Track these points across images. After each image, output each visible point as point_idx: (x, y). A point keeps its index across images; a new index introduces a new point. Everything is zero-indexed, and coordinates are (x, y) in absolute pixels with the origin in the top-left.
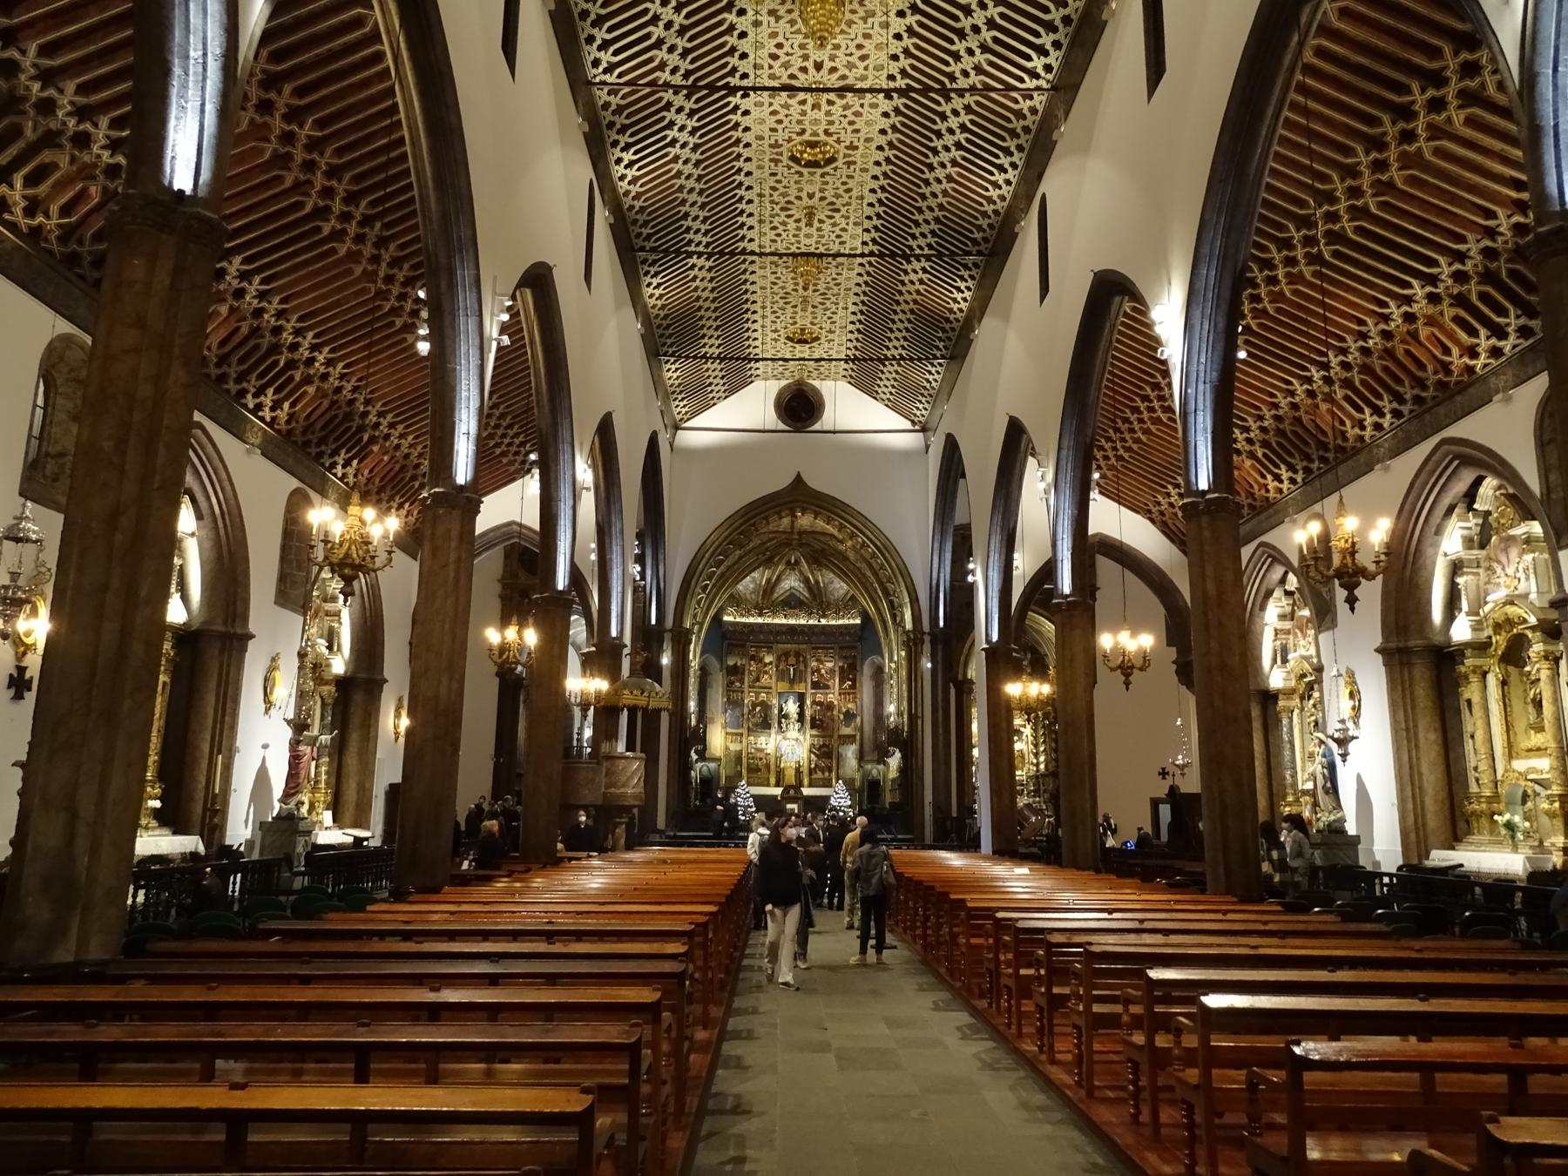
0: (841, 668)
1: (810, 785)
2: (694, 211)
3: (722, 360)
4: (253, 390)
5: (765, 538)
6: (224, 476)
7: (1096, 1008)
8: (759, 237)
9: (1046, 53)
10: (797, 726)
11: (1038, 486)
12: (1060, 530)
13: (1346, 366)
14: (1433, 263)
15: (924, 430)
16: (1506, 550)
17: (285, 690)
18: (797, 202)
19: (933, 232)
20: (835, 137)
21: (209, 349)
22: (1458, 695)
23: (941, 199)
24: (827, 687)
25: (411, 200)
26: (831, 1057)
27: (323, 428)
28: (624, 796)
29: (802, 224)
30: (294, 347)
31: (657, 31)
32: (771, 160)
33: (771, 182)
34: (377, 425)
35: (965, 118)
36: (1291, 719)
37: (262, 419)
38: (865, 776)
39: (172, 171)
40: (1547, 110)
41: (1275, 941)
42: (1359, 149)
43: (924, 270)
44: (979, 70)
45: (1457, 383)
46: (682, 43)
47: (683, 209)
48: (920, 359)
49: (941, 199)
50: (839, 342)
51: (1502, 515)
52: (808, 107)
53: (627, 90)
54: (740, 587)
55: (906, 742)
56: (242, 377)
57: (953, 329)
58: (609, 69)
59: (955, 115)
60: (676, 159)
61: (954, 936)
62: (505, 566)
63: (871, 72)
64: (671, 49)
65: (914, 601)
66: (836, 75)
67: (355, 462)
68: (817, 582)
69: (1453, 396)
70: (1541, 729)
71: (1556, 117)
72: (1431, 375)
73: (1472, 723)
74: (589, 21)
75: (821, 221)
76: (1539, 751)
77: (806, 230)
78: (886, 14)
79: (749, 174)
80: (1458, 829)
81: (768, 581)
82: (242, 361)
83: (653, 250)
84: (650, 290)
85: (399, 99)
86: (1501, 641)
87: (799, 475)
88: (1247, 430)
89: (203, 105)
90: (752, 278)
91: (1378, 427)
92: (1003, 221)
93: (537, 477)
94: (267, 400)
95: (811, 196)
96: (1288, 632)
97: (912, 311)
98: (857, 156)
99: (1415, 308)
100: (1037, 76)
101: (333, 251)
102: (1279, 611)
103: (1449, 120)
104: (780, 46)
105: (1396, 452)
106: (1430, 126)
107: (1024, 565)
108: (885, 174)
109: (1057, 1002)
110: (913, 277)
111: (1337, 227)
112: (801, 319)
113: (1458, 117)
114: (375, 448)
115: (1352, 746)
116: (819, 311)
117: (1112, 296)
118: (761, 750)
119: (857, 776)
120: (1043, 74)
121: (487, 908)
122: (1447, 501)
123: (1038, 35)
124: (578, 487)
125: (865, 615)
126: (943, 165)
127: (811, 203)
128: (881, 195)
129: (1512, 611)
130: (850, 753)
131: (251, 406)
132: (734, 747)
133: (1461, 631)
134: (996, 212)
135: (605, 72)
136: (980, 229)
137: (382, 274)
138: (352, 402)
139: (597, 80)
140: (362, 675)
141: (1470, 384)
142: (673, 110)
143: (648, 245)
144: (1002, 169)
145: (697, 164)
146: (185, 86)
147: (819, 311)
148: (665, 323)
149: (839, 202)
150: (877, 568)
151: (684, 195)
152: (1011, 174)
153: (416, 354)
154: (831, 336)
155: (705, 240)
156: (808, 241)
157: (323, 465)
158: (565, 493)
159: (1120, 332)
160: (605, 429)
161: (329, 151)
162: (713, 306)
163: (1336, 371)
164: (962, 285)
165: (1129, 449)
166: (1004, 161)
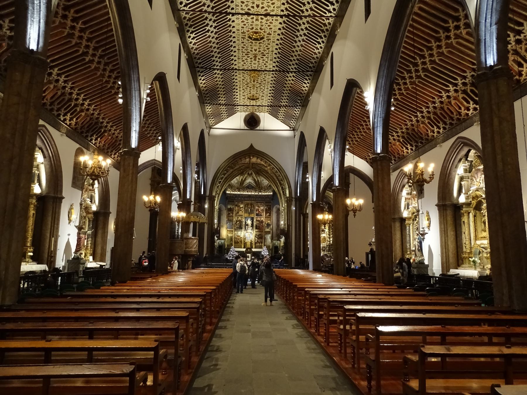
0: (266, 209)
1: (255, 248)
2: (216, 55)
3: (226, 105)
4: (63, 114)
5: (240, 165)
6: (53, 143)
7: (331, 318)
8: (238, 64)
10: (251, 228)
11: (329, 149)
12: (335, 165)
13: (429, 112)
14: (456, 79)
15: (294, 130)
16: (477, 173)
17: (75, 216)
19: (296, 64)
20: (263, 30)
21: (47, 100)
22: (461, 220)
23: (299, 53)
24: (261, 215)
25: (116, 50)
26: (250, 334)
27: (88, 127)
28: (191, 251)
29: (253, 60)
30: (77, 99)
33: (242, 45)
34: (106, 126)
35: (307, 25)
36: (409, 227)
37: (66, 124)
38: (273, 244)
39: (29, 43)
40: (482, 34)
41: (389, 297)
42: (433, 41)
43: (294, 76)
44: (311, 9)
45: (463, 119)
48: (292, 106)
49: (299, 53)
50: (265, 99)
51: (476, 162)
52: (254, 20)
53: (192, 13)
54: (232, 182)
55: (286, 233)
56: (59, 110)
57: (303, 96)
59: (304, 24)
60: (209, 37)
61: (294, 296)
62: (152, 174)
63: (275, 9)
65: (290, 187)
66: (264, 9)
67: (99, 139)
68: (258, 180)
69: (462, 123)
70: (485, 231)
71: (485, 36)
72: (455, 116)
73: (465, 229)
75: (259, 59)
76: (484, 238)
77: (254, 62)
79: (234, 42)
80: (459, 262)
81: (242, 180)
82: (58, 104)
83: (202, 68)
84: (201, 81)
85: (111, 15)
86: (474, 202)
87: (252, 146)
88: (397, 132)
89: (40, 20)
90: (236, 78)
91: (438, 132)
92: (320, 60)
93: (161, 145)
94: (68, 117)
95: (255, 50)
96: (409, 199)
97: (290, 90)
98: (271, 37)
99: (450, 94)
100: (331, 12)
101: (90, 67)
102: (407, 192)
103: (461, 33)
105: (444, 141)
106: (455, 34)
107: (325, 176)
108: (280, 43)
109: (320, 316)
110: (290, 78)
111: (425, 67)
112: (252, 92)
113: (464, 32)
114: (106, 134)
115: (426, 236)
116: (259, 89)
117: (352, 87)
118: (239, 236)
119: (271, 245)
121: (140, 288)
122: (459, 157)
124: (175, 148)
125: (274, 192)
126: (300, 41)
127: (255, 53)
129: (477, 193)
130: (269, 237)
131: (62, 119)
132: (230, 235)
133: (462, 199)
134: (317, 57)
135: (184, 6)
136: (312, 63)
137: (107, 75)
138: (98, 118)
139: (182, 9)
140: (103, 211)
141: (468, 119)
142: (208, 20)
143: (200, 66)
144: (319, 43)
145: (217, 38)
146: (33, 13)
147: (259, 89)
148: (206, 92)
149: (265, 52)
150: (278, 176)
151: (212, 49)
152: (322, 45)
153: (118, 103)
154: (263, 98)
155: (220, 64)
156: (255, 66)
157: (88, 140)
158: (171, 150)
159: (356, 99)
160: (185, 128)
161: (87, 32)
162: (222, 87)
163: (425, 114)
164: (306, 82)
165: (360, 138)
166: (320, 40)
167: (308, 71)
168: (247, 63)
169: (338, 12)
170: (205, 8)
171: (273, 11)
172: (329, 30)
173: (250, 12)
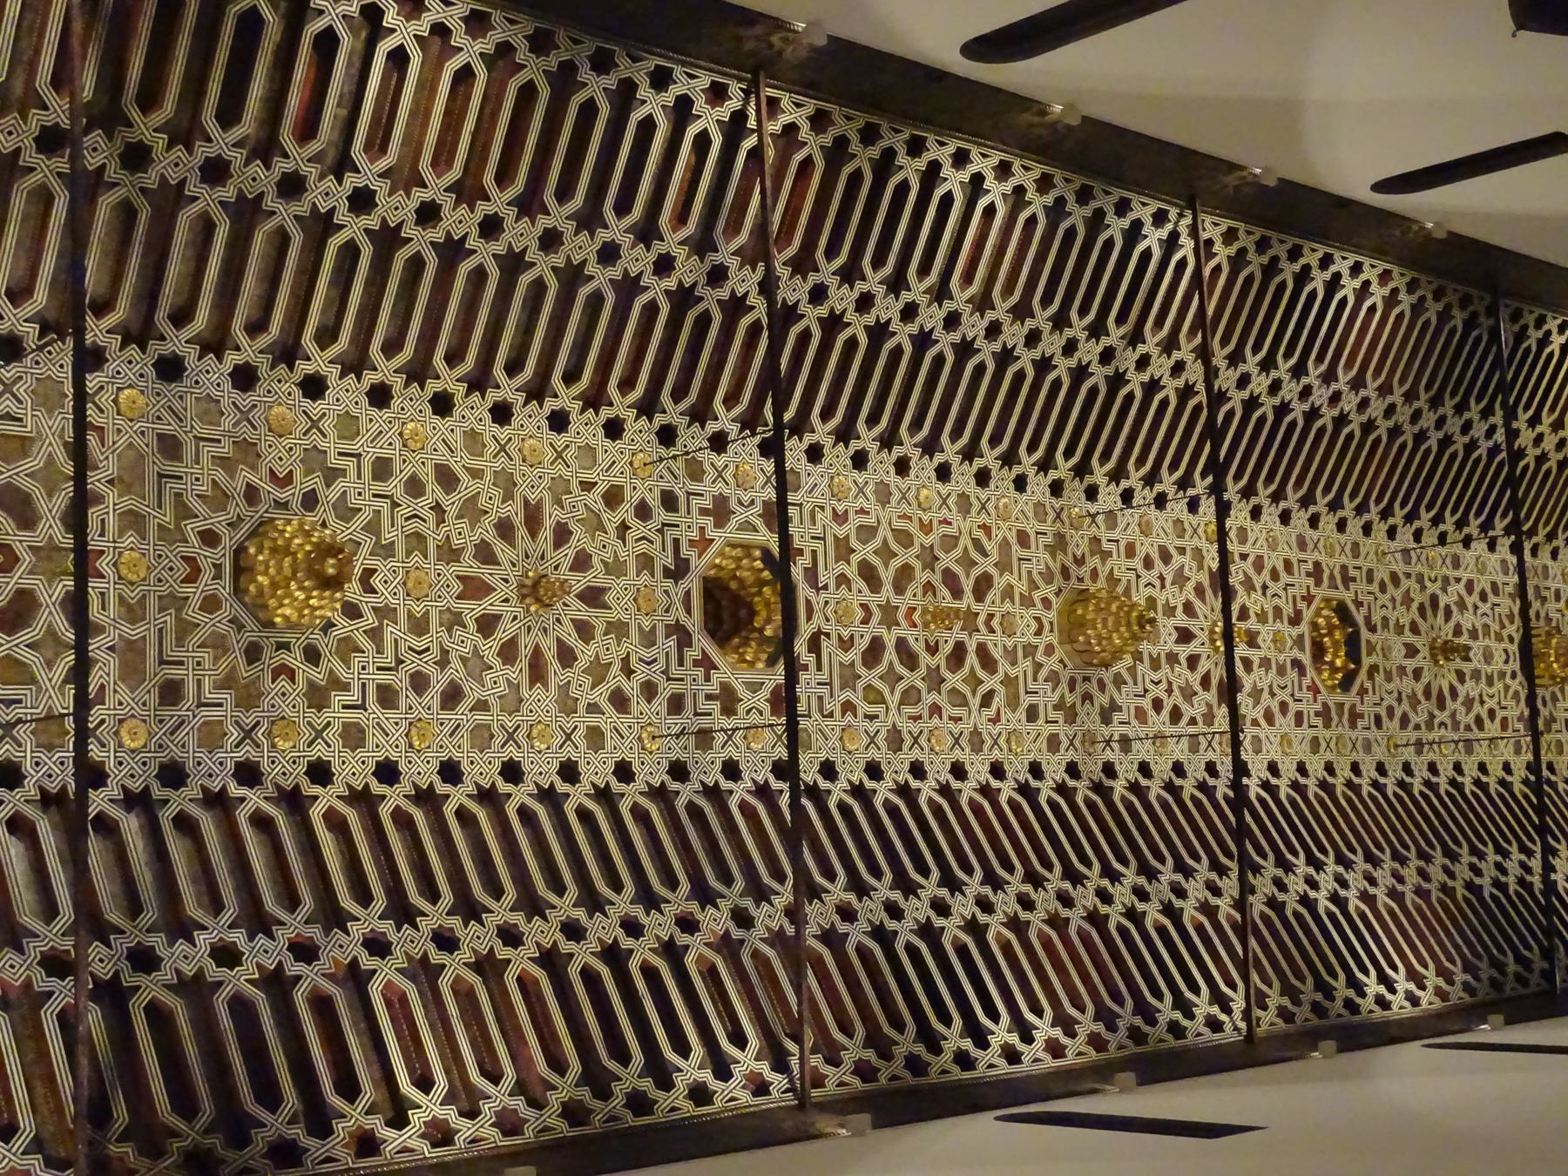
8: (1504, 756)
9: (1137, 225)
18: (1425, 680)
19: (1460, 408)
20: (1302, 605)
23: (1397, 397)
31: (1153, 914)
32: (1353, 726)
43: (1534, 421)
44: (1170, 345)
46: (1168, 874)
47: (1461, 892)
49: (1397, 397)
52: (1255, 655)
53: (1255, 977)
58: (1224, 1004)
59: (1251, 381)
64: (1180, 893)
66: (1197, 603)
74: (1147, 1029)
77: (1477, 662)
78: (1093, 516)
79: (1381, 769)
83: (1548, 954)
100: (1174, 236)
104: (1157, 705)
120: (1170, 226)
123: (1109, 244)
126: (1335, 398)
127: (1424, 652)
128: (1398, 518)
134: (1412, 287)
135: (1227, 1010)
136: (1444, 316)
139: (1242, 1025)
142: (1281, 897)
143: (1539, 964)
144: (1334, 284)
149: (1418, 598)
155: (1517, 855)
156: (1499, 657)
166: (1318, 282)
167: (1494, 333)
168: (1491, 703)
169: (1170, 194)
170: (1224, 905)
171: (1198, 555)
172: (1259, 232)
173: (1218, 673)
